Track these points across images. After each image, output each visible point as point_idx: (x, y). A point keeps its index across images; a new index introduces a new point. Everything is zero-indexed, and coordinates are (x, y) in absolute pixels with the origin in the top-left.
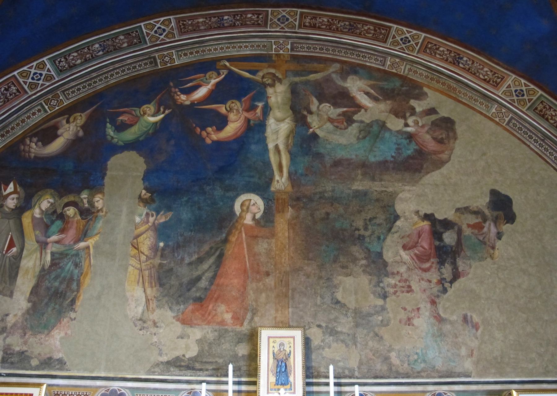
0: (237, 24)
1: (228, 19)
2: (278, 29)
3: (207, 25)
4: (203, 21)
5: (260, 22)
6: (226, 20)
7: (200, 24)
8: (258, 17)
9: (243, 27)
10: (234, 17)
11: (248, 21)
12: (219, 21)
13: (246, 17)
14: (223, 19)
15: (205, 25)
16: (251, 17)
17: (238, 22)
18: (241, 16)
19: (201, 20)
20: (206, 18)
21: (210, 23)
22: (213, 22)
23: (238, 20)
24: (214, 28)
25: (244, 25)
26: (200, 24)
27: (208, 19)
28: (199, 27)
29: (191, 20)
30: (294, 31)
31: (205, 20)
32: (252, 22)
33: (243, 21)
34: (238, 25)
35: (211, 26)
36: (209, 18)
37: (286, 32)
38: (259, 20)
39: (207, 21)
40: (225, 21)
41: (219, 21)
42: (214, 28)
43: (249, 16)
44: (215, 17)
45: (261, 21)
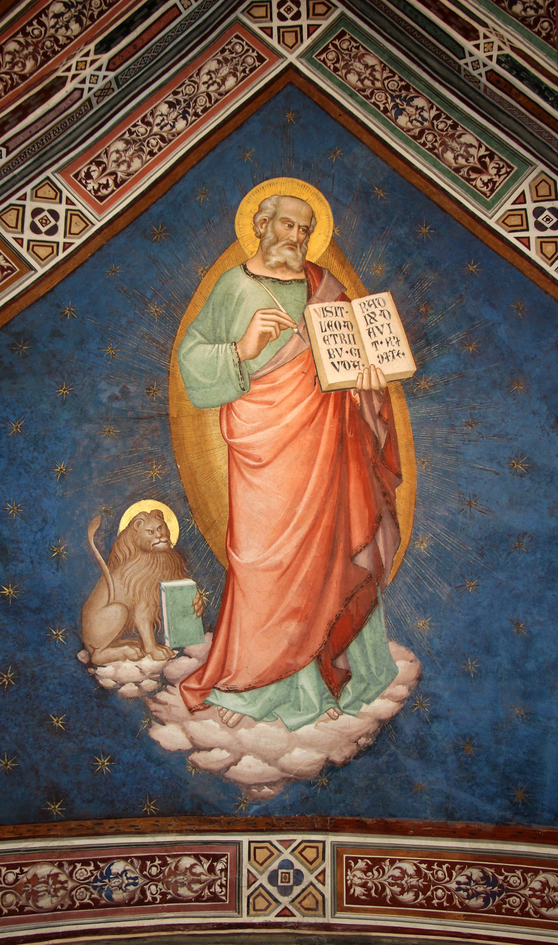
0: (149, 898)
1: (125, 871)
2: (272, 918)
3: (61, 893)
4: (49, 876)
5: (218, 889)
6: (118, 875)
7: (41, 887)
8: (211, 869)
9: (169, 910)
10: (143, 868)
11: (183, 884)
12: (96, 880)
13: (176, 867)
14: (109, 871)
15: (56, 890)
16: (193, 866)
17: (153, 888)
18: (165, 864)
19: (44, 870)
20: (61, 865)
21: (70, 885)
22: (80, 884)
23: (152, 879)
24: (84, 906)
25: (172, 900)
26: (41, 887)
27: (66, 866)
28: (35, 896)
29: (14, 867)
30: (320, 920)
31: (56, 870)
32: (196, 887)
33: (168, 884)
34: (155, 899)
35: (71, 898)
36: (71, 863)
37: (297, 926)
38: (214, 881)
39: (62, 878)
40: (115, 882)
41: (96, 880)
42: (84, 906)
43: (187, 862)
44: (85, 863)
45: (221, 886)
